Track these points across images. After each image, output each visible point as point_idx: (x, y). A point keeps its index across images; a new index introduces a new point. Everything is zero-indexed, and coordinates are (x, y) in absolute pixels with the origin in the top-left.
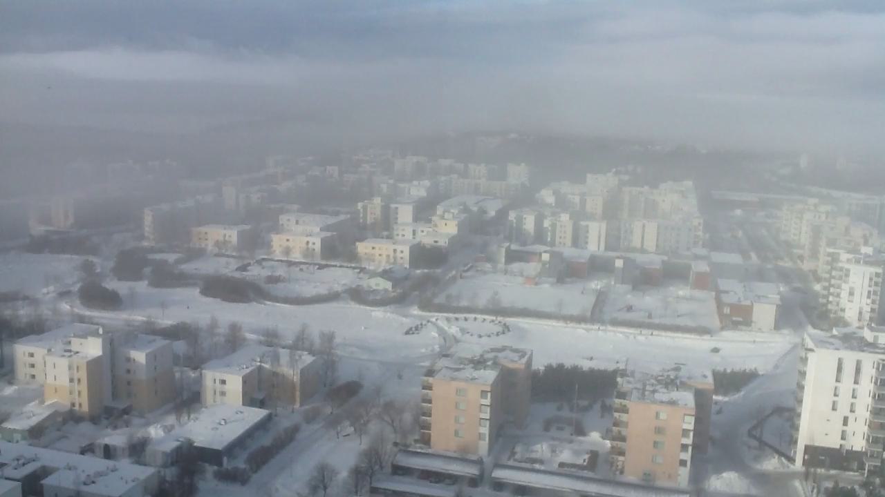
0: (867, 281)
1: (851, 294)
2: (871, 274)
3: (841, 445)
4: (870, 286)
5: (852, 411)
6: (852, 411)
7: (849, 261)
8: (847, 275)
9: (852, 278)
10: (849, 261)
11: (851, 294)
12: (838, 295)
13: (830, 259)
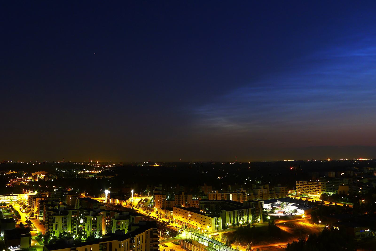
2: (63, 218)
7: (55, 215)
9: (56, 221)
13: (48, 215)
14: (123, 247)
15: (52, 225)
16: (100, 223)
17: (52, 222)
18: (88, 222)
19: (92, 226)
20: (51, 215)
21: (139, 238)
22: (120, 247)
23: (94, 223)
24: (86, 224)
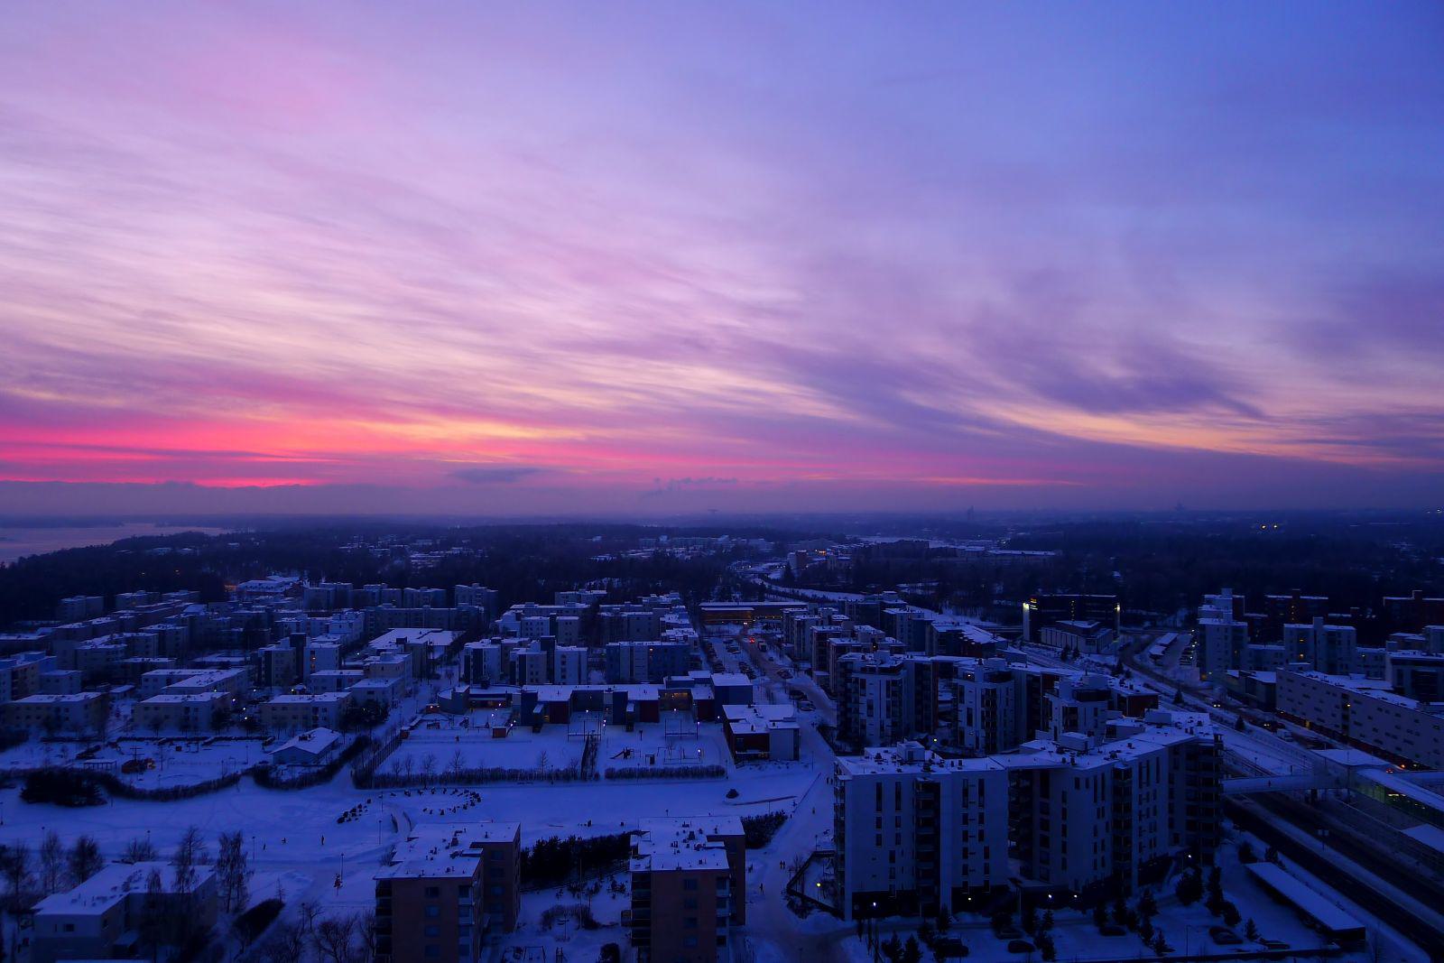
0: (884, 693)
1: (870, 707)
2: (888, 682)
3: (890, 886)
4: (888, 696)
5: (898, 842)
6: (898, 842)
7: (864, 670)
8: (863, 686)
9: (869, 689)
10: (864, 670)
11: (870, 707)
12: (857, 711)
14: (1087, 786)
15: (857, 702)
16: (1007, 704)
17: (857, 691)
18: (967, 698)
19: (982, 712)
20: (851, 671)
21: (1144, 765)
22: (1077, 786)
23: (988, 704)
24: (961, 707)
